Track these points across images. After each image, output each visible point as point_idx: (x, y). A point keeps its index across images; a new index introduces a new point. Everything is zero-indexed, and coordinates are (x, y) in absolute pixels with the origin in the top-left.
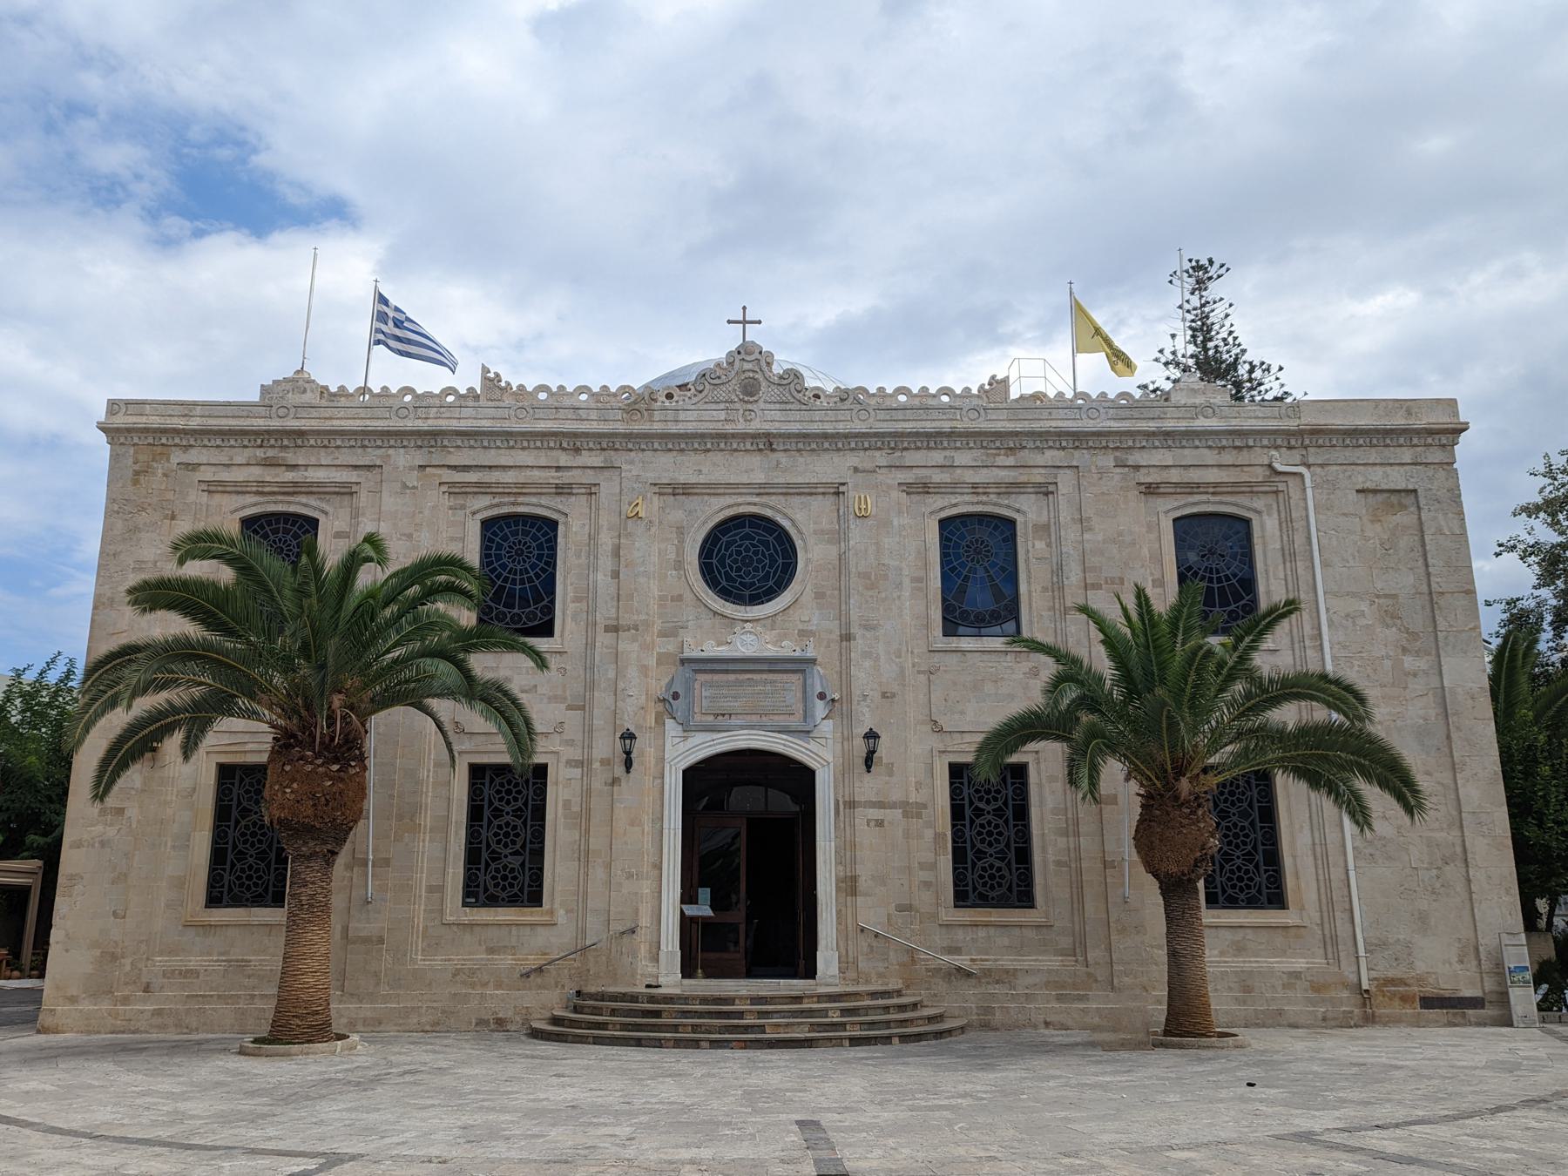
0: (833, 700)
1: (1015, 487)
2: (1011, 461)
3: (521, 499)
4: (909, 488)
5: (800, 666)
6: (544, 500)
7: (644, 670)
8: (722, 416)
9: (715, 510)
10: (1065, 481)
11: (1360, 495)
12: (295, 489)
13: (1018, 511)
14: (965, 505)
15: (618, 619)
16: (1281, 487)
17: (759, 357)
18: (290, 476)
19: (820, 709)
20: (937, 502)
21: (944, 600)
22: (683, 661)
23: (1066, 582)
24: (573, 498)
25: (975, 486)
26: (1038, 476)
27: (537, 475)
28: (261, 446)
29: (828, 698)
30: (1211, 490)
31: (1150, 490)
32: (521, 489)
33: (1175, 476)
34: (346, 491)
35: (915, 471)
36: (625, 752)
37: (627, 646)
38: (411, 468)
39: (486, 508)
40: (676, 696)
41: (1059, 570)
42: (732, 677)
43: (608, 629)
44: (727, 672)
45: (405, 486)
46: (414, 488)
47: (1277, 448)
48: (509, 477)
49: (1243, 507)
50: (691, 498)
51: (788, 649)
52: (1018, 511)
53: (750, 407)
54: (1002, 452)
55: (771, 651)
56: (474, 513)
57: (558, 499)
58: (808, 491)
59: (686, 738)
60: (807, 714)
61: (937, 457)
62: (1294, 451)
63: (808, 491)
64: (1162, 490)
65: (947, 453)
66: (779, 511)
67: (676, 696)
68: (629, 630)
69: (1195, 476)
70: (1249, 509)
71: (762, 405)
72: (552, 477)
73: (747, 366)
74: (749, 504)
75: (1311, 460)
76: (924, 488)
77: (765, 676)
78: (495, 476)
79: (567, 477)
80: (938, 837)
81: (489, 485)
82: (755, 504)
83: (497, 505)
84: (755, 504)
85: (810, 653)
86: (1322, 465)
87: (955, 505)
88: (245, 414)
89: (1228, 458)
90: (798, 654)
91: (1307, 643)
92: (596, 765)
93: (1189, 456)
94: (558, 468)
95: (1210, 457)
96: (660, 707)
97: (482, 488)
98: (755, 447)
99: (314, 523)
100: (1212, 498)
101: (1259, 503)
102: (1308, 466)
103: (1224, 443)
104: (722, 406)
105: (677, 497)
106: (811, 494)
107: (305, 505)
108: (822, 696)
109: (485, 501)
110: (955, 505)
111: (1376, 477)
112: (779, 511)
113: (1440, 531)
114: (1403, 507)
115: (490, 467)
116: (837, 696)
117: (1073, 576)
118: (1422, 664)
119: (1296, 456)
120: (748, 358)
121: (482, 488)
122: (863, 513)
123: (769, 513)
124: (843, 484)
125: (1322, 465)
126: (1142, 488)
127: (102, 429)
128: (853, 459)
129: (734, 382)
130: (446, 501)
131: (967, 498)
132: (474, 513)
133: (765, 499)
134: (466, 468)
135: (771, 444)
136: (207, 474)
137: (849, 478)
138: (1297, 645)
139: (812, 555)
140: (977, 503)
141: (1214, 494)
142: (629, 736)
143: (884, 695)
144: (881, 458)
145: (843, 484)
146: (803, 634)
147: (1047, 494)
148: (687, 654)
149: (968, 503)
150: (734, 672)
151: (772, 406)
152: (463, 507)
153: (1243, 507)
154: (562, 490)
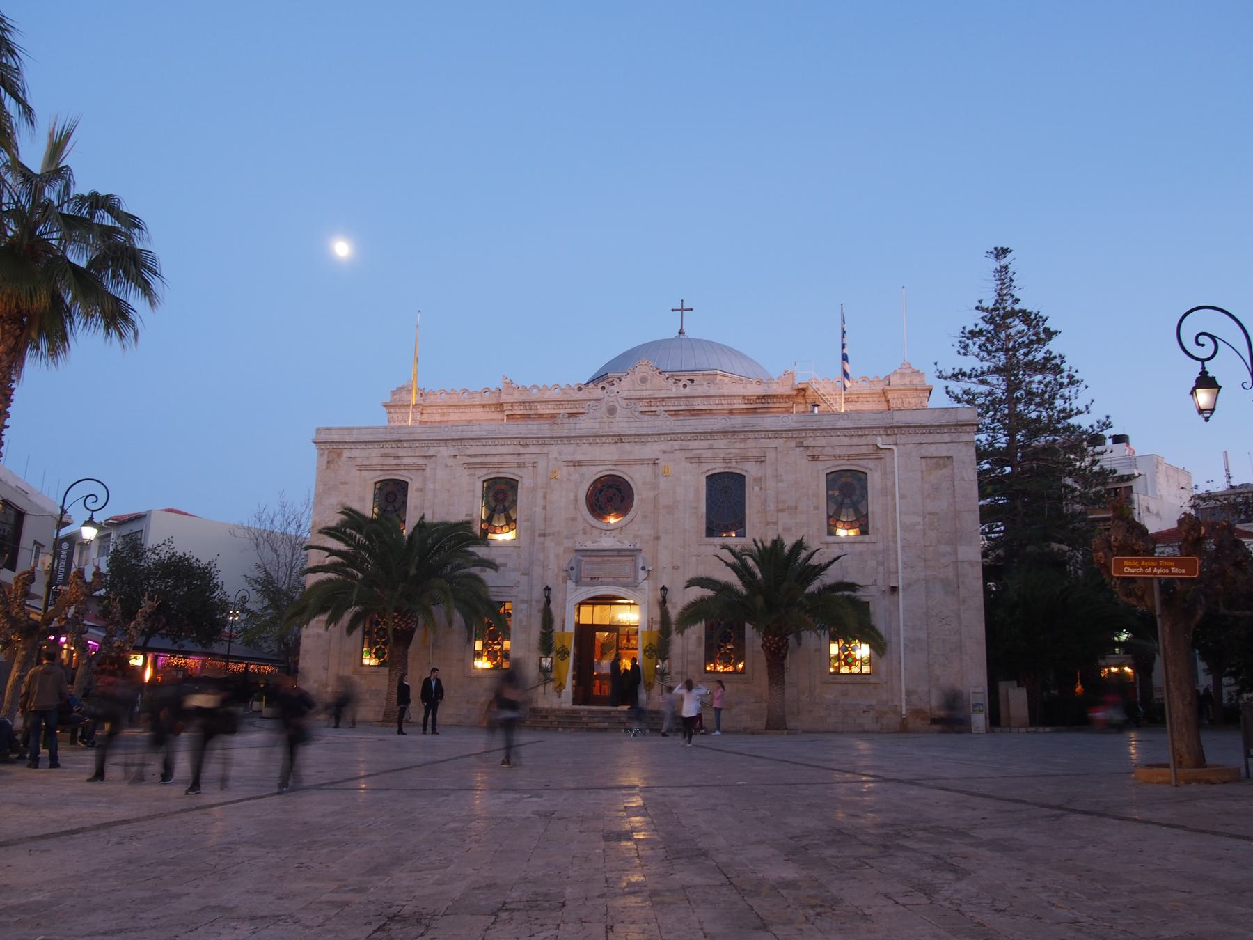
0: (649, 570)
1: (745, 458)
2: (742, 445)
3: (501, 470)
4: (690, 460)
5: (632, 553)
6: (512, 470)
7: (557, 556)
8: (598, 425)
9: (594, 473)
10: (771, 455)
11: (923, 460)
12: (398, 467)
13: (746, 471)
14: (720, 468)
15: (545, 530)
16: (883, 456)
17: (617, 394)
18: (395, 462)
19: (642, 574)
20: (706, 467)
21: (708, 518)
22: (577, 551)
23: (768, 509)
24: (525, 469)
25: (724, 459)
26: (756, 453)
27: (509, 459)
28: (382, 448)
29: (647, 569)
30: (846, 458)
31: (814, 458)
32: (500, 465)
33: (828, 451)
34: (421, 468)
35: (694, 451)
36: (546, 597)
37: (549, 543)
38: (450, 457)
39: (485, 475)
40: (572, 569)
41: (764, 503)
42: (600, 559)
43: (540, 535)
44: (597, 556)
45: (447, 466)
46: (451, 466)
47: (880, 435)
48: (495, 460)
49: (863, 467)
50: (583, 467)
51: (627, 545)
52: (746, 471)
53: (611, 420)
54: (739, 440)
55: (619, 546)
56: (479, 478)
57: (518, 469)
58: (641, 462)
59: (577, 589)
60: (636, 578)
61: (705, 444)
62: (890, 437)
63: (641, 462)
64: (820, 459)
65: (710, 442)
66: (625, 474)
67: (572, 569)
68: (550, 535)
69: (838, 451)
70: (866, 468)
71: (617, 419)
72: (514, 459)
73: (611, 399)
74: (611, 470)
75: (898, 442)
76: (699, 460)
77: (616, 558)
78: (488, 460)
79: (522, 459)
80: (699, 638)
81: (486, 464)
82: (613, 470)
83: (490, 474)
84: (613, 470)
85: (638, 546)
86: (904, 444)
87: (714, 469)
88: (375, 432)
89: (855, 441)
90: (632, 547)
91: (890, 538)
92: (534, 603)
93: (835, 440)
94: (519, 454)
95: (846, 441)
96: (565, 574)
97: (483, 466)
98: (614, 441)
99: (408, 483)
100: (846, 462)
101: (871, 464)
102: (896, 444)
103: (853, 433)
104: (598, 420)
105: (577, 467)
106: (642, 464)
107: (402, 476)
108: (643, 568)
109: (485, 471)
110: (714, 469)
111: (932, 450)
112: (625, 474)
113: (963, 479)
114: (945, 466)
115: (486, 455)
116: (650, 569)
117: (772, 506)
118: (949, 549)
119: (891, 439)
120: (611, 395)
121: (483, 466)
122: (666, 474)
123: (621, 475)
124: (657, 459)
125: (904, 444)
126: (810, 458)
127: (315, 443)
128: (663, 446)
129: (604, 408)
130: (466, 472)
131: (720, 465)
132: (479, 478)
133: (619, 468)
134: (475, 456)
135: (621, 440)
136: (359, 461)
137: (659, 455)
138: (885, 540)
139: (641, 495)
140: (726, 467)
141: (848, 460)
142: (548, 589)
143: (673, 568)
144: (676, 445)
145: (657, 459)
146: (635, 536)
147: (762, 462)
148: (577, 548)
149: (720, 467)
150: (600, 556)
151: (622, 420)
152: (474, 475)
153: (863, 467)
154: (520, 465)
